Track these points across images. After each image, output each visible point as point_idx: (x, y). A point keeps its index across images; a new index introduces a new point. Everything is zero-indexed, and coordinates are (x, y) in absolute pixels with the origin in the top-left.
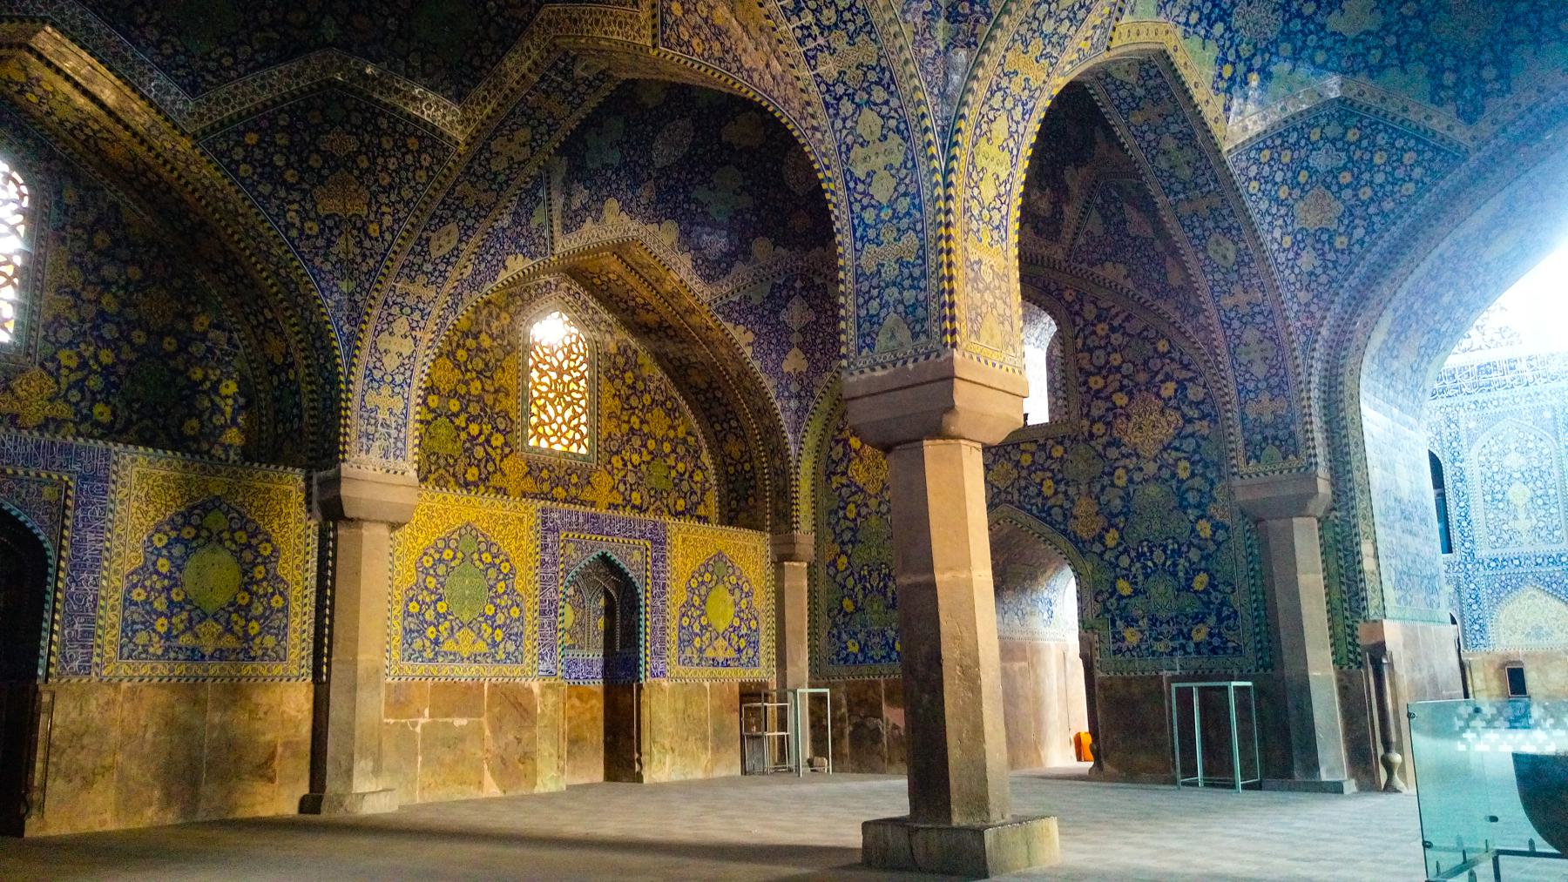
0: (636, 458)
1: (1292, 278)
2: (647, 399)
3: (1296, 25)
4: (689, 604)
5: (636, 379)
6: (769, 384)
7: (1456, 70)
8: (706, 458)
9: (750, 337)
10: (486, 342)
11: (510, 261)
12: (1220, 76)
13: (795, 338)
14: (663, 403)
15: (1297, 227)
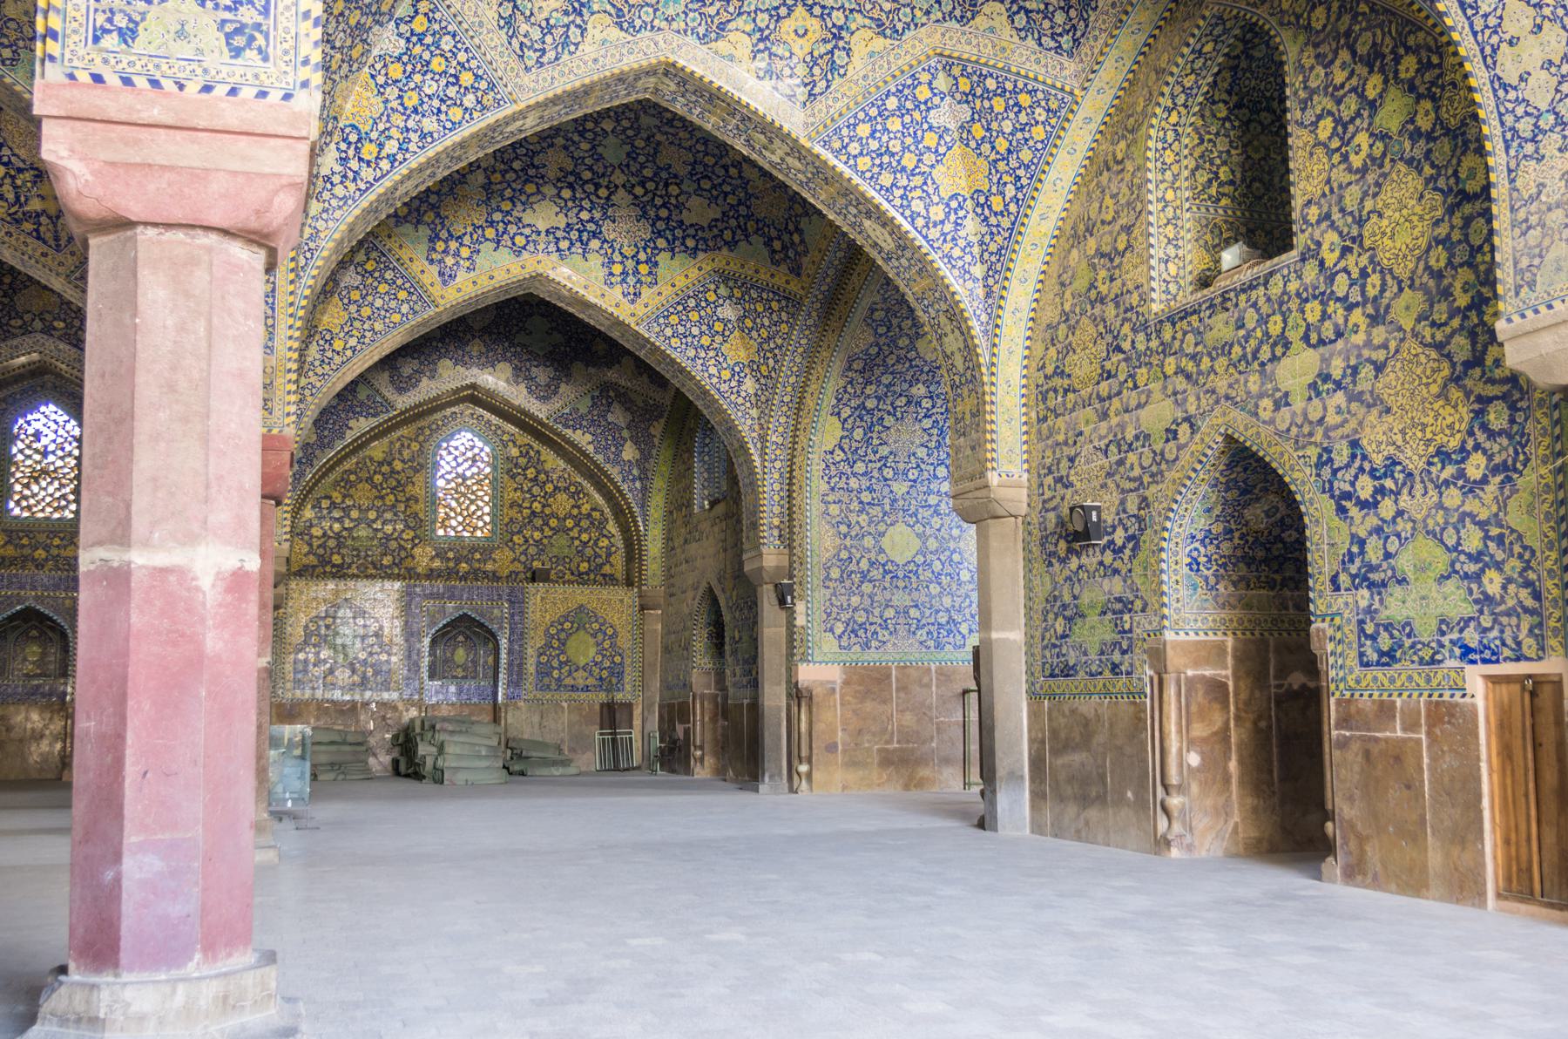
0: (537, 535)
1: (740, 401)
2: (549, 488)
3: (661, 225)
4: (549, 645)
5: (538, 472)
6: (614, 471)
7: (779, 238)
8: (612, 527)
9: (589, 437)
10: (398, 465)
11: (352, 423)
12: (611, 274)
13: (625, 433)
14: (566, 489)
15: (731, 363)
